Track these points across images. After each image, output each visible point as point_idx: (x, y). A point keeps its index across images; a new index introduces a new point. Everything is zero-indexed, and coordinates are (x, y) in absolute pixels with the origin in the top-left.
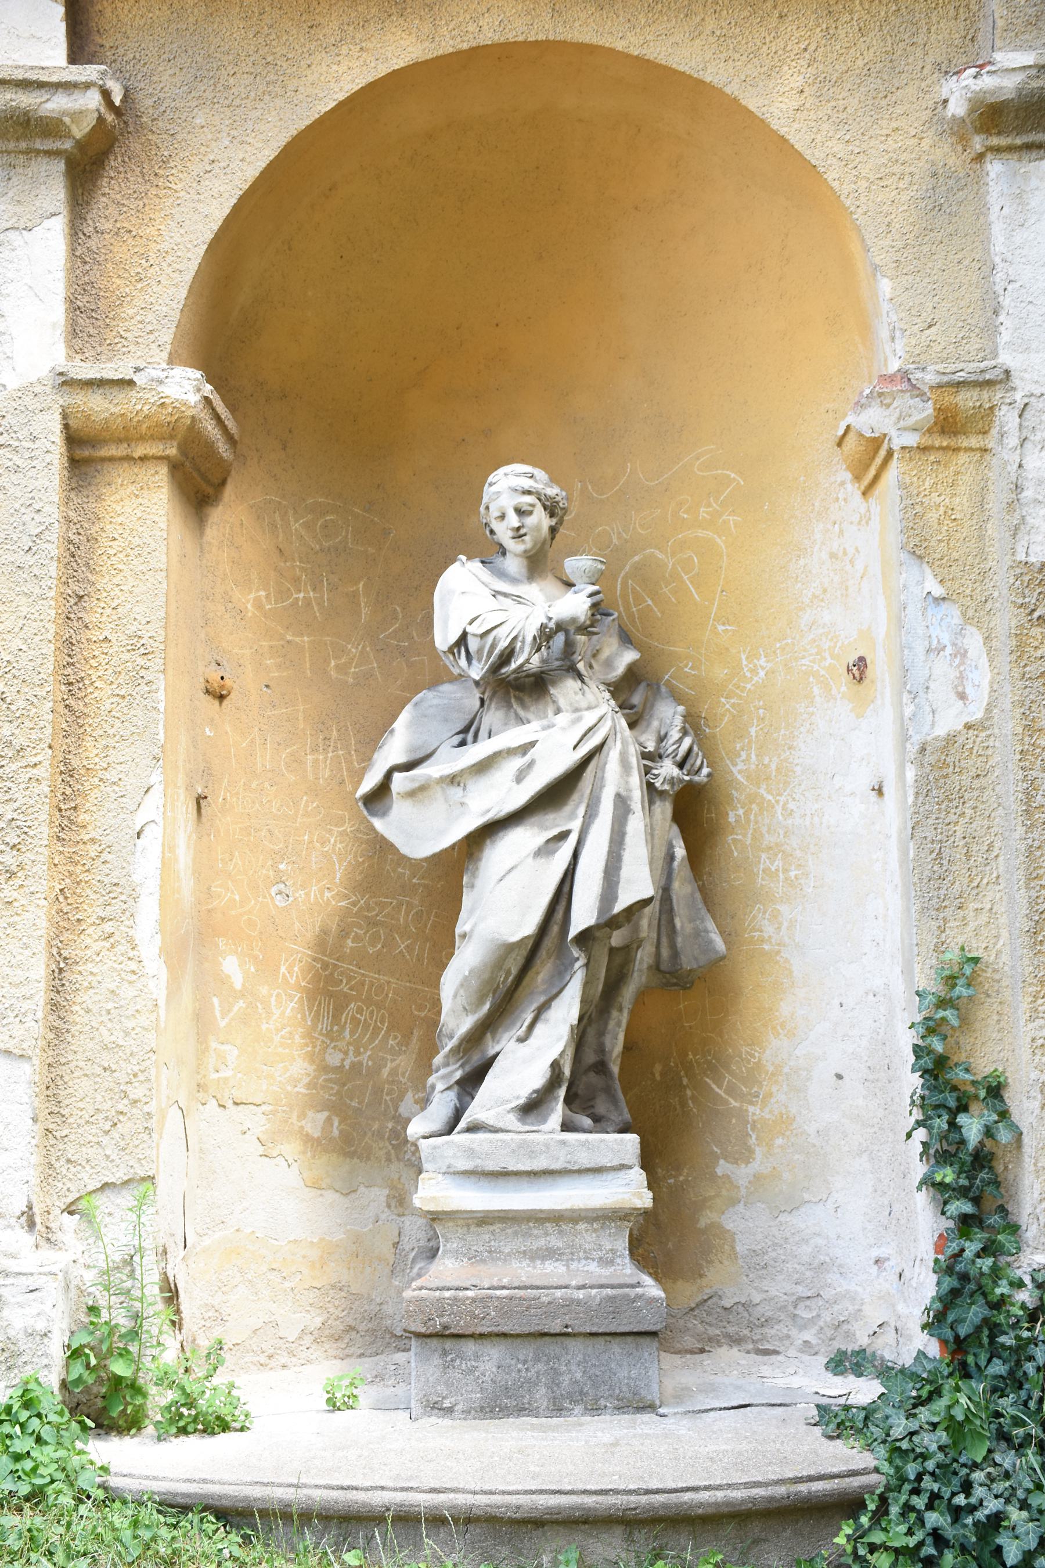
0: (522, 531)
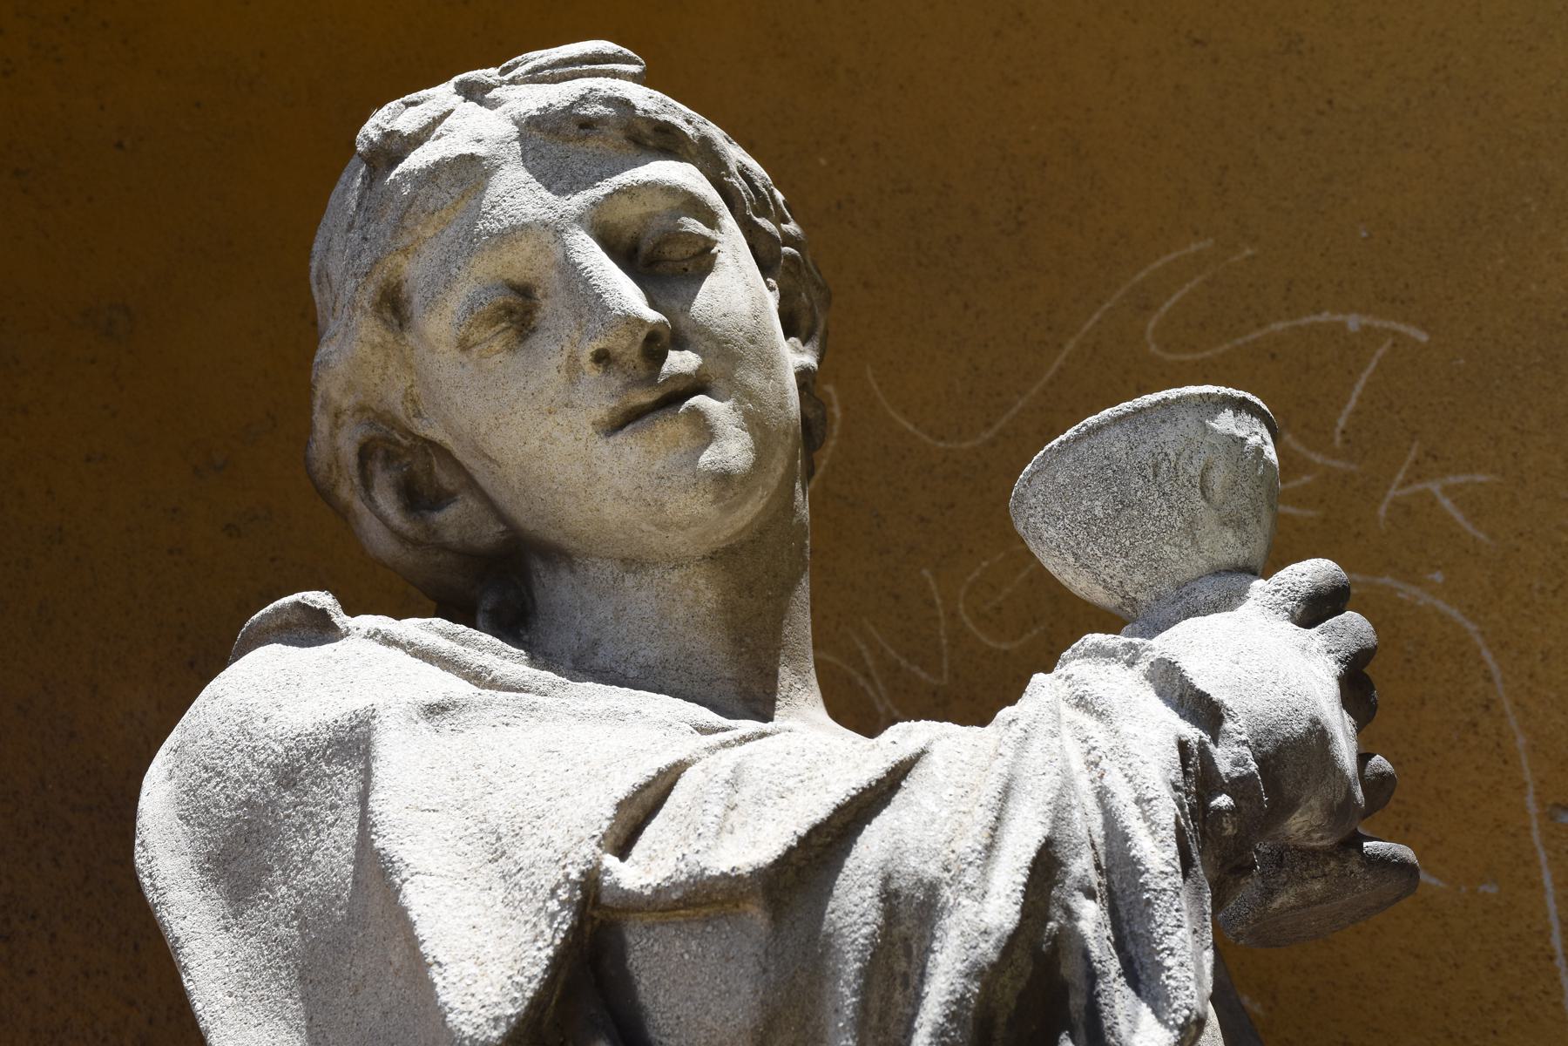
0: (681, 361)
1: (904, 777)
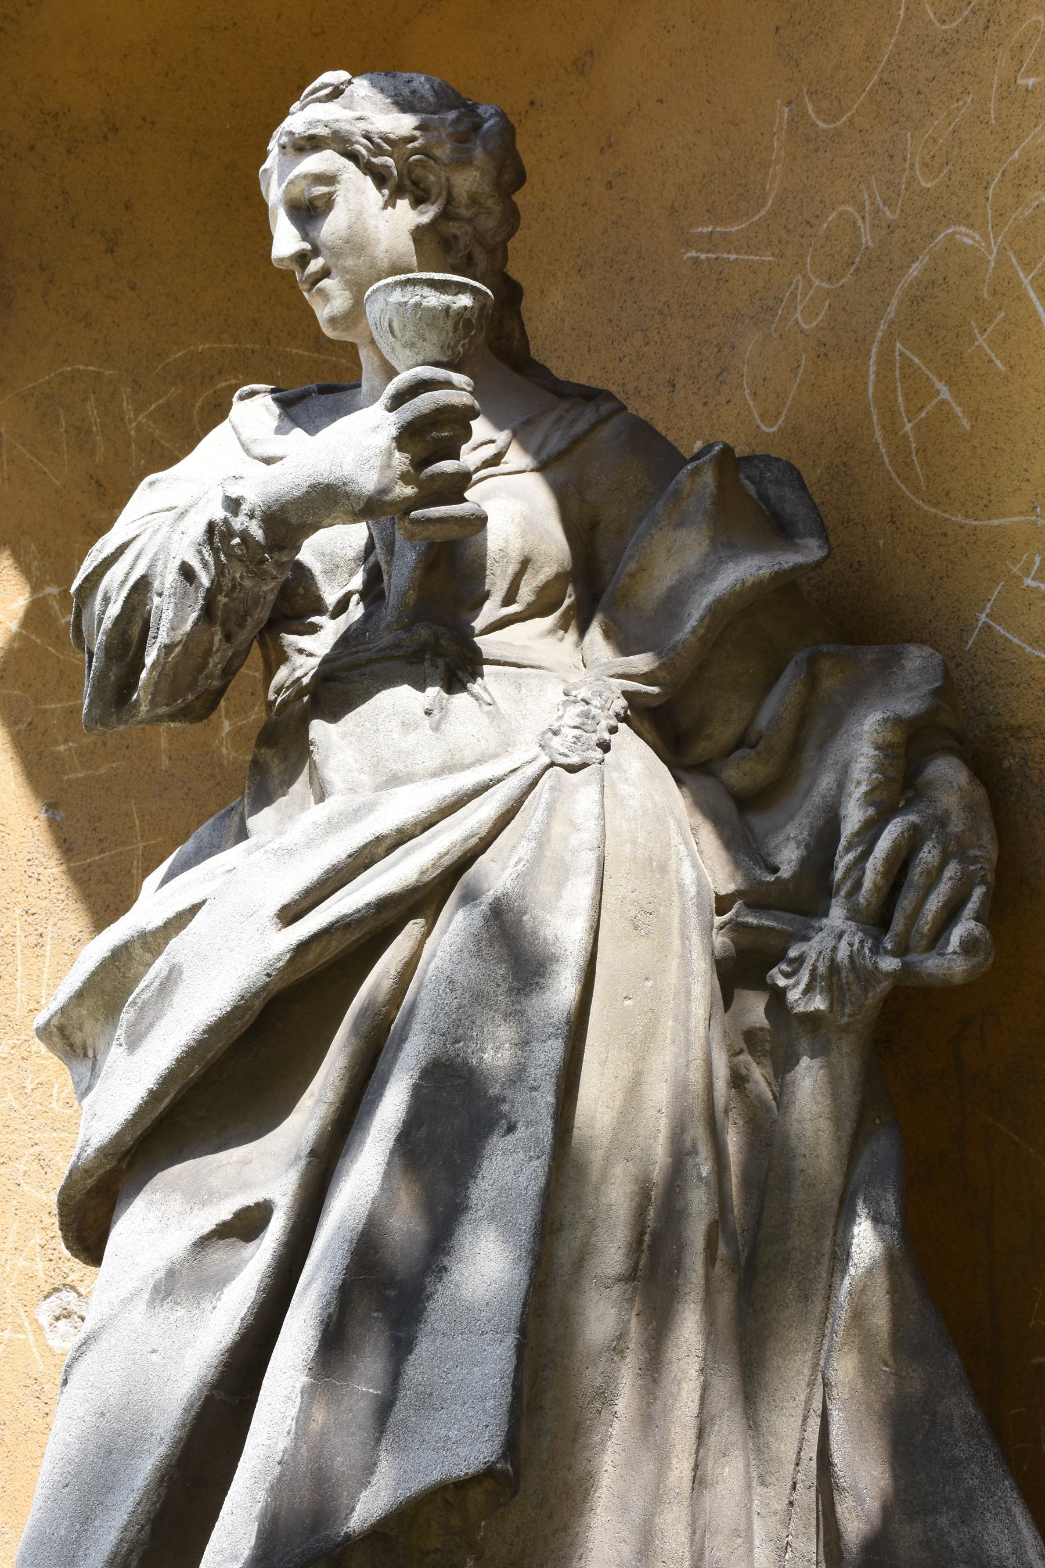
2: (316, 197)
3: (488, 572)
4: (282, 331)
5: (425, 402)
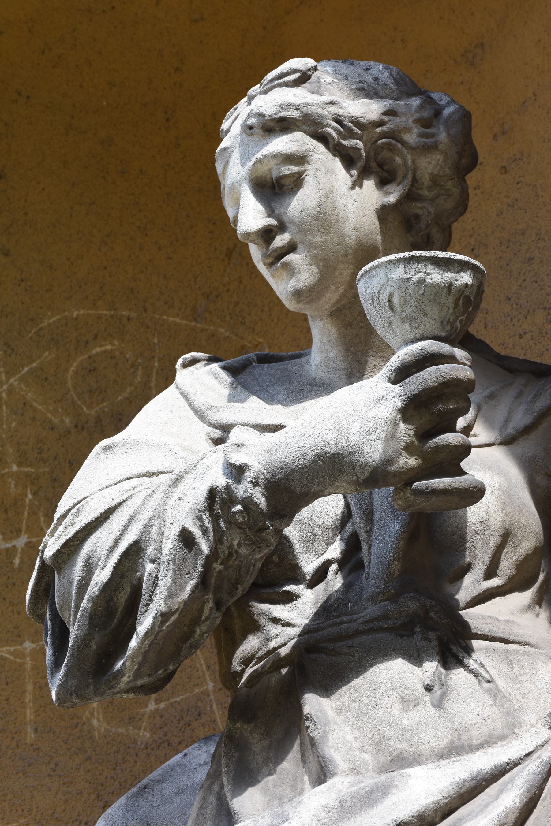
0: (281, 240)
1: (111, 514)
2: (285, 176)
3: (468, 545)
4: (158, 300)
5: (432, 375)
